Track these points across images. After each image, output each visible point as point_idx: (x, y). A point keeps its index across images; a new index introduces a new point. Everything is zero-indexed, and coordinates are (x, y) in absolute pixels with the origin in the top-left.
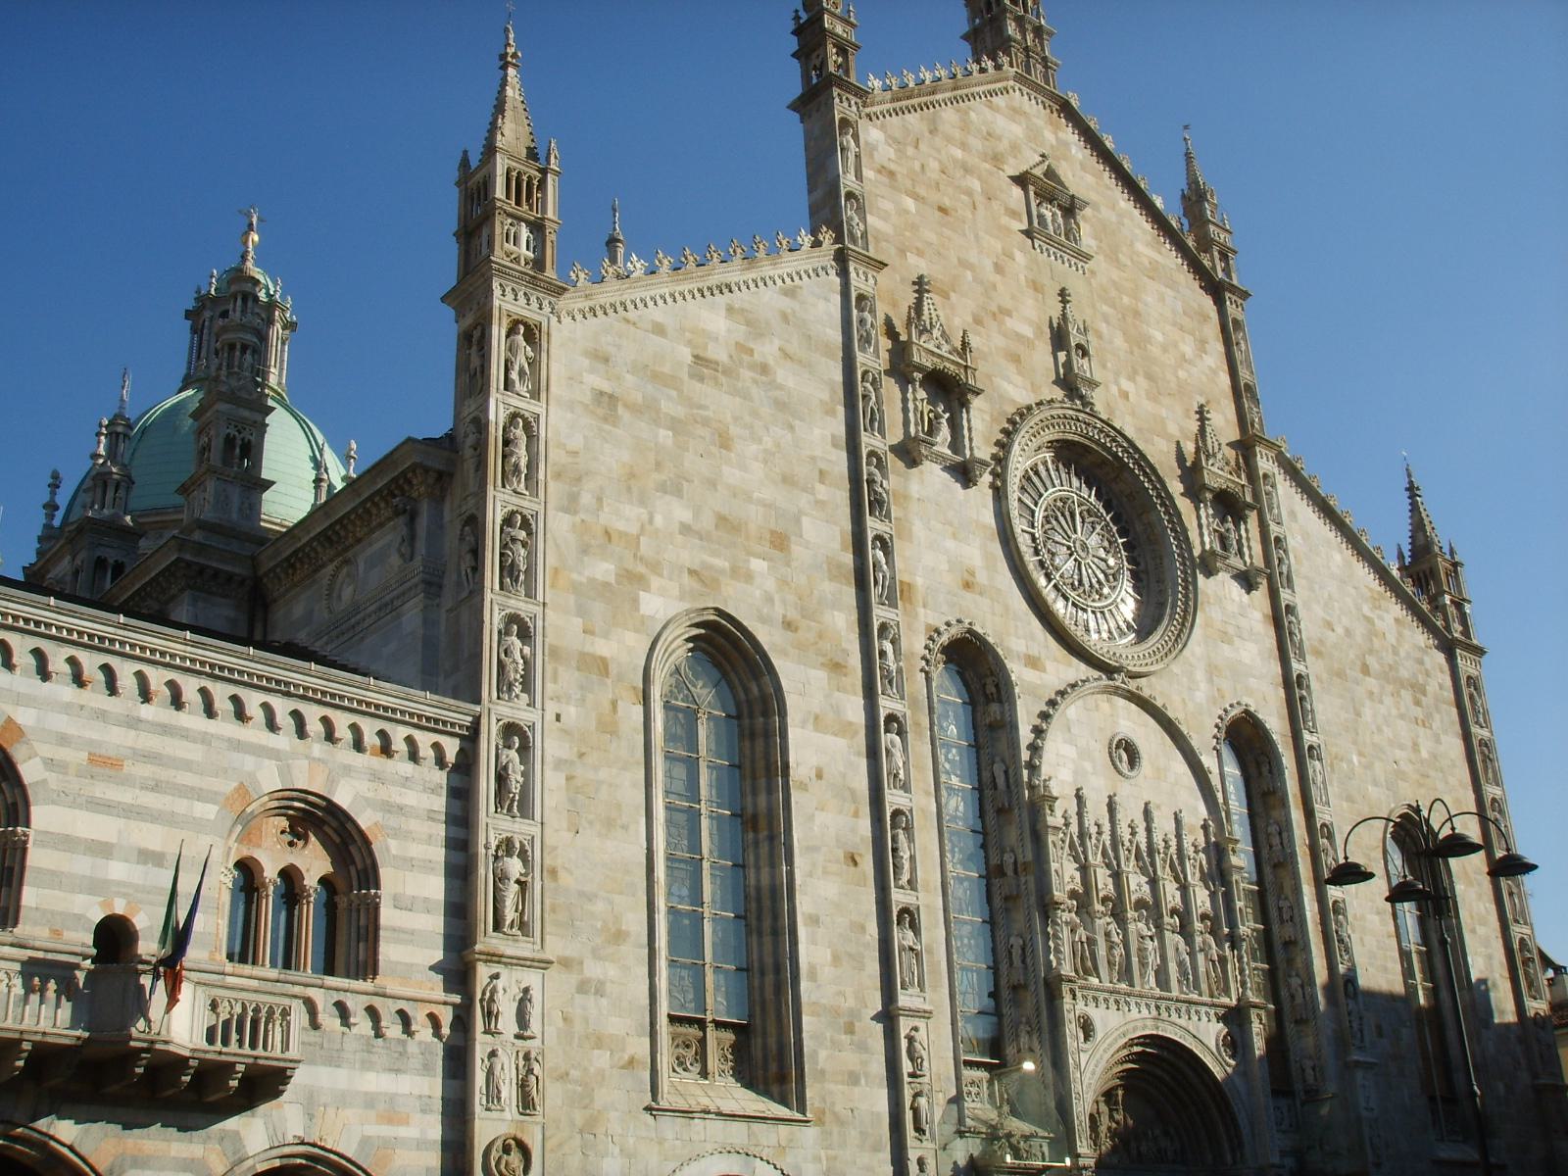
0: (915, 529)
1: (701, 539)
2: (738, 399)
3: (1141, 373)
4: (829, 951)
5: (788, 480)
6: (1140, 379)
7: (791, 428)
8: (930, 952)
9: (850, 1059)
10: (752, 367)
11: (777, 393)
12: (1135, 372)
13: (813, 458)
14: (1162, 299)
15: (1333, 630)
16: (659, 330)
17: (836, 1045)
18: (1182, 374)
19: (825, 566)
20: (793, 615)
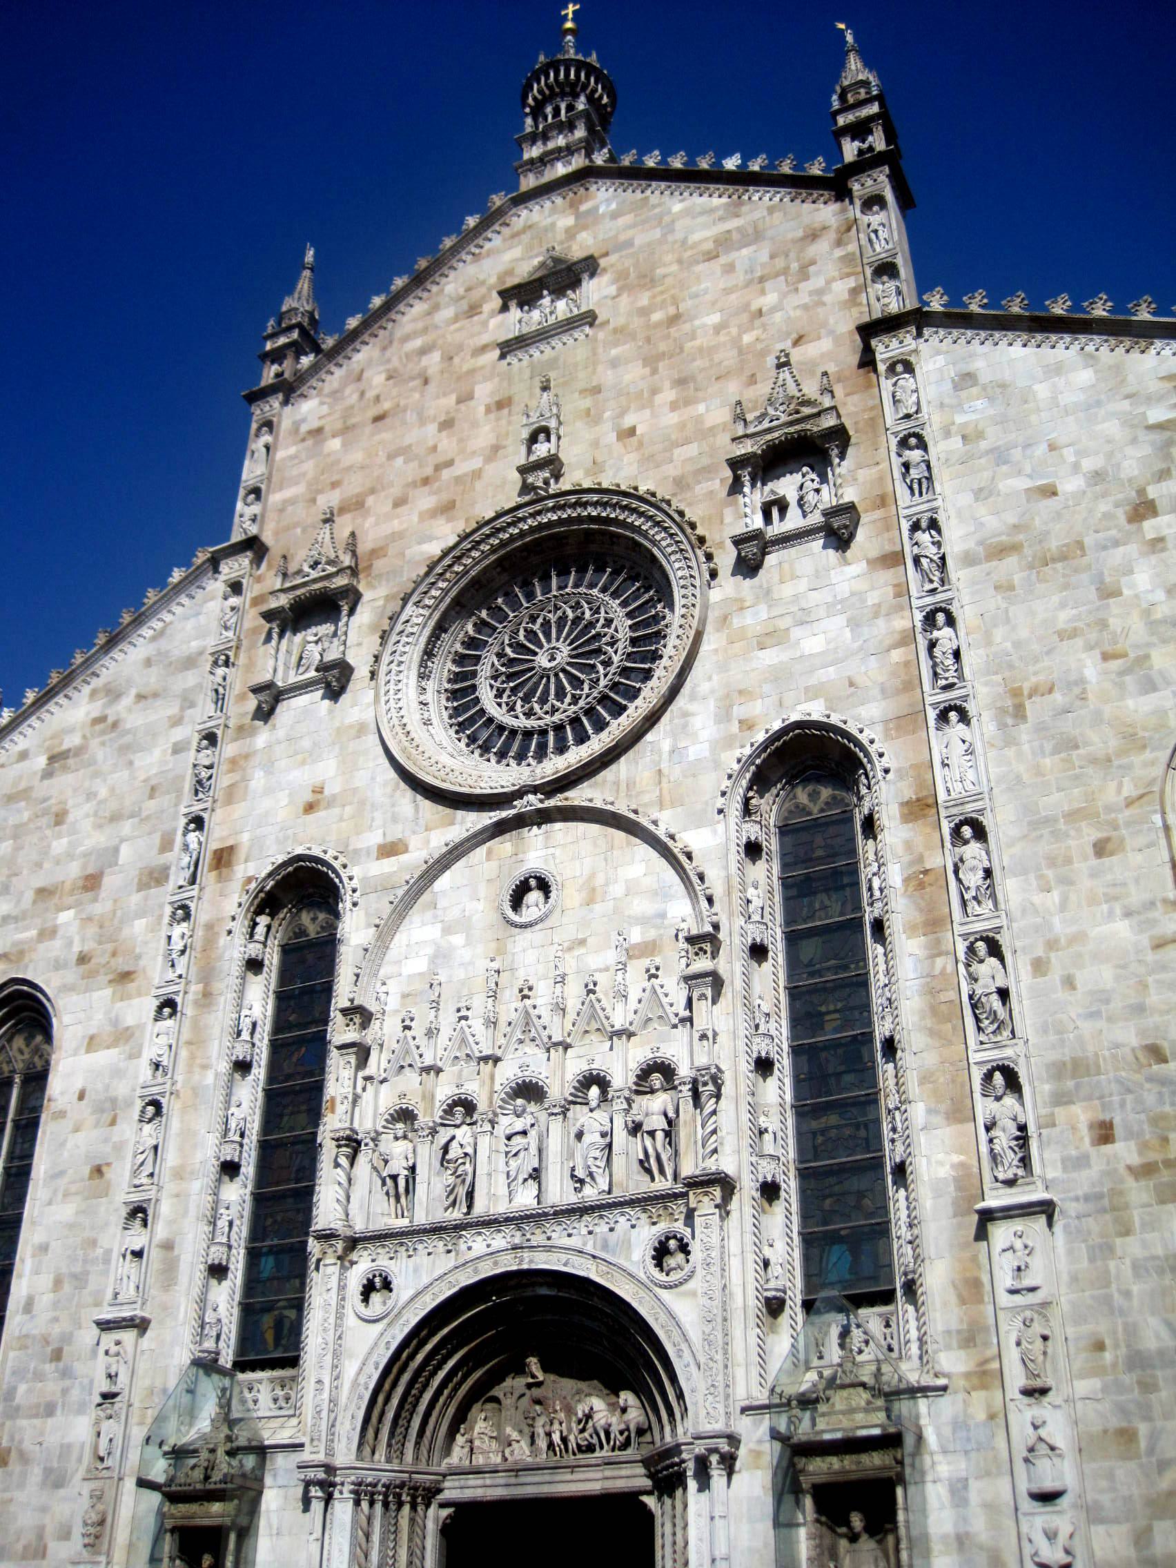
0: (253, 784)
1: (16, 919)
2: (82, 771)
3: (667, 384)
4: (52, 1276)
5: (115, 818)
6: (668, 395)
7: (131, 763)
8: (168, 1246)
9: (52, 1387)
10: (103, 733)
11: (128, 739)
12: (654, 391)
13: (144, 781)
14: (730, 269)
15: (1055, 494)
16: (24, 755)
17: (39, 1376)
18: (747, 339)
19: (136, 880)
20: (89, 946)
